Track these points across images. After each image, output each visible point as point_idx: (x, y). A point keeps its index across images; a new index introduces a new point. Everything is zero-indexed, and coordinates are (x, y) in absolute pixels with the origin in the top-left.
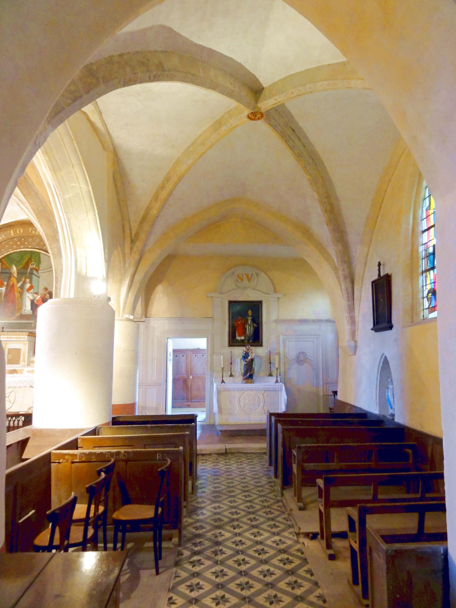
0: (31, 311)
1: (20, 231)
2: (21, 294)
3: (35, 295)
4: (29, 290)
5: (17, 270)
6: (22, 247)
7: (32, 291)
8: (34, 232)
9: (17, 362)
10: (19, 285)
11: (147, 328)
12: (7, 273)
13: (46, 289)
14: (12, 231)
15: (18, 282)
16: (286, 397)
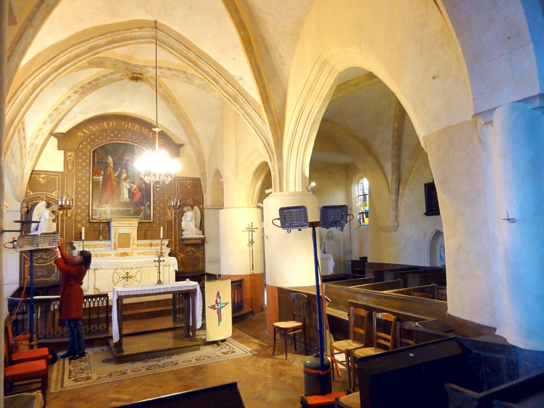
0: (129, 199)
1: (113, 124)
2: (119, 183)
3: (132, 185)
4: (125, 179)
5: (113, 161)
6: (116, 139)
7: (128, 180)
8: (126, 126)
9: (128, 246)
10: (116, 174)
12: (104, 163)
14: (105, 123)
15: (115, 172)
16: (334, 263)
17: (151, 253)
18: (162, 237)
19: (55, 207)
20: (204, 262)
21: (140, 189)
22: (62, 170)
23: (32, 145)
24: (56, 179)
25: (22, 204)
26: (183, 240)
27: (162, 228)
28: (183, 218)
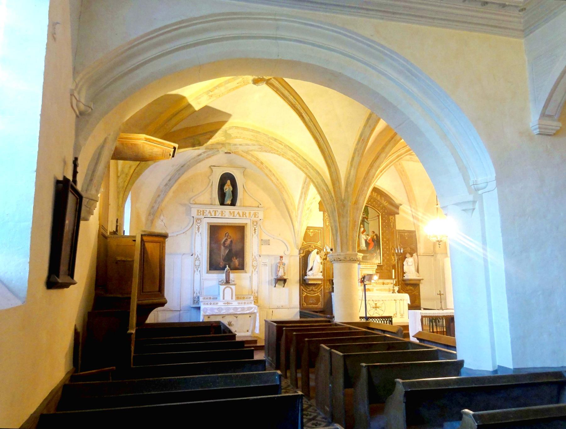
4: (363, 233)
11: (435, 260)
13: (374, 232)
17: (385, 290)
18: (393, 277)
19: (323, 253)
20: (419, 299)
21: (373, 240)
22: (322, 226)
23: (308, 208)
24: (318, 233)
25: (300, 251)
26: (404, 280)
27: (393, 270)
28: (405, 263)
